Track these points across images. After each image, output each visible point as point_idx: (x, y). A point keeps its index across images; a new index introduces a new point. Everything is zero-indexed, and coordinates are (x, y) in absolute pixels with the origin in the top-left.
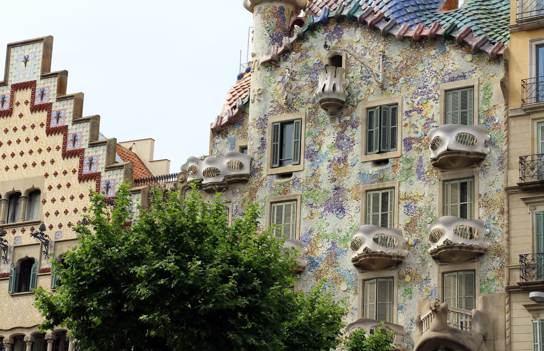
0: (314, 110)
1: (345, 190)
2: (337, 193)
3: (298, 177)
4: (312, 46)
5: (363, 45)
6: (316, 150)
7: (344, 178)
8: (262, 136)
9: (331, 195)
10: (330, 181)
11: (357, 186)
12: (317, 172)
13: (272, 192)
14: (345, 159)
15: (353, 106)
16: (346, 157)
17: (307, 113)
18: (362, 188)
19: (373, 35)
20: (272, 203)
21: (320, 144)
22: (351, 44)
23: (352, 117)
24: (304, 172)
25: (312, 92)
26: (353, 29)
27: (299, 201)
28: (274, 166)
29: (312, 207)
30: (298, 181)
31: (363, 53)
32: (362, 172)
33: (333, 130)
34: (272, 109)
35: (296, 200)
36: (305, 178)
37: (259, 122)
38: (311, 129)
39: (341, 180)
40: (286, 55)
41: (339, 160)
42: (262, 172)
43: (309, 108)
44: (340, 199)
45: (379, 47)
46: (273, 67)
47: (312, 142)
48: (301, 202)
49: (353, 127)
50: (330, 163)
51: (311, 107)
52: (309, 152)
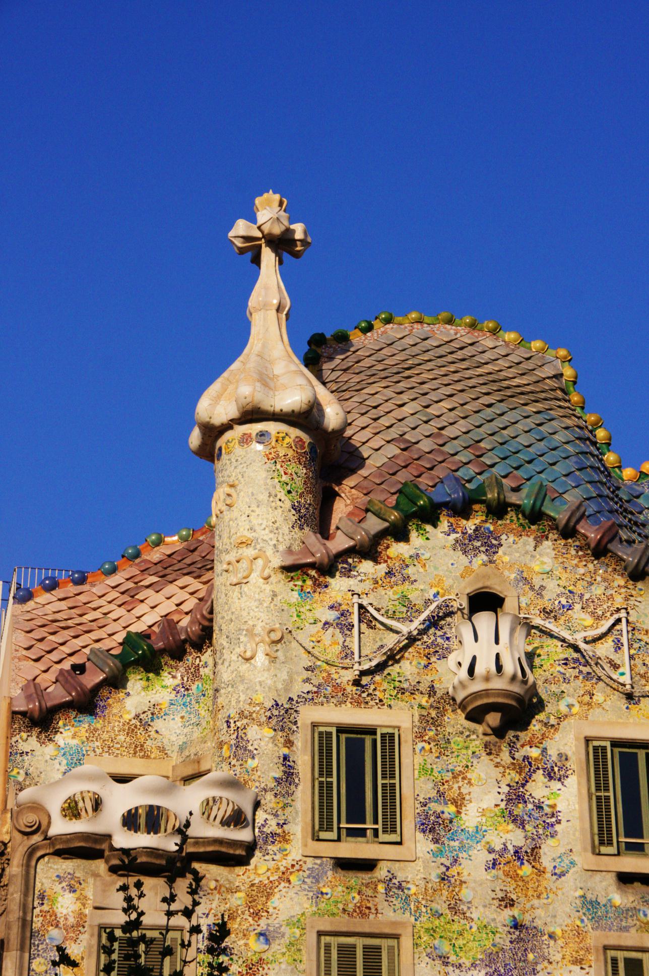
0: (433, 713)
1: (543, 934)
2: (520, 940)
3: (400, 876)
4: (417, 555)
5: (562, 583)
6: (446, 816)
7: (536, 902)
8: (286, 751)
9: (504, 939)
10: (496, 903)
11: (579, 933)
12: (453, 871)
13: (322, 906)
14: (534, 853)
15: (546, 724)
16: (535, 849)
17: (416, 718)
18: (595, 938)
19: (591, 566)
20: (320, 934)
21: (459, 802)
22: (525, 575)
23: (544, 750)
24: (419, 865)
25: (426, 667)
26: (531, 541)
27: (406, 942)
28: (323, 835)
29: (446, 964)
30: (400, 887)
31: (564, 601)
32: (589, 896)
33: (496, 773)
34: (308, 687)
35: (397, 937)
36: (422, 883)
37: (276, 713)
38: (429, 761)
39: (528, 906)
40: (350, 561)
41: (516, 852)
42: (287, 847)
43: (421, 707)
44: (531, 956)
45: (610, 598)
46: (309, 582)
47: (433, 794)
48: (416, 945)
49: (551, 778)
50: (492, 856)
51: (424, 703)
52: (427, 817)
